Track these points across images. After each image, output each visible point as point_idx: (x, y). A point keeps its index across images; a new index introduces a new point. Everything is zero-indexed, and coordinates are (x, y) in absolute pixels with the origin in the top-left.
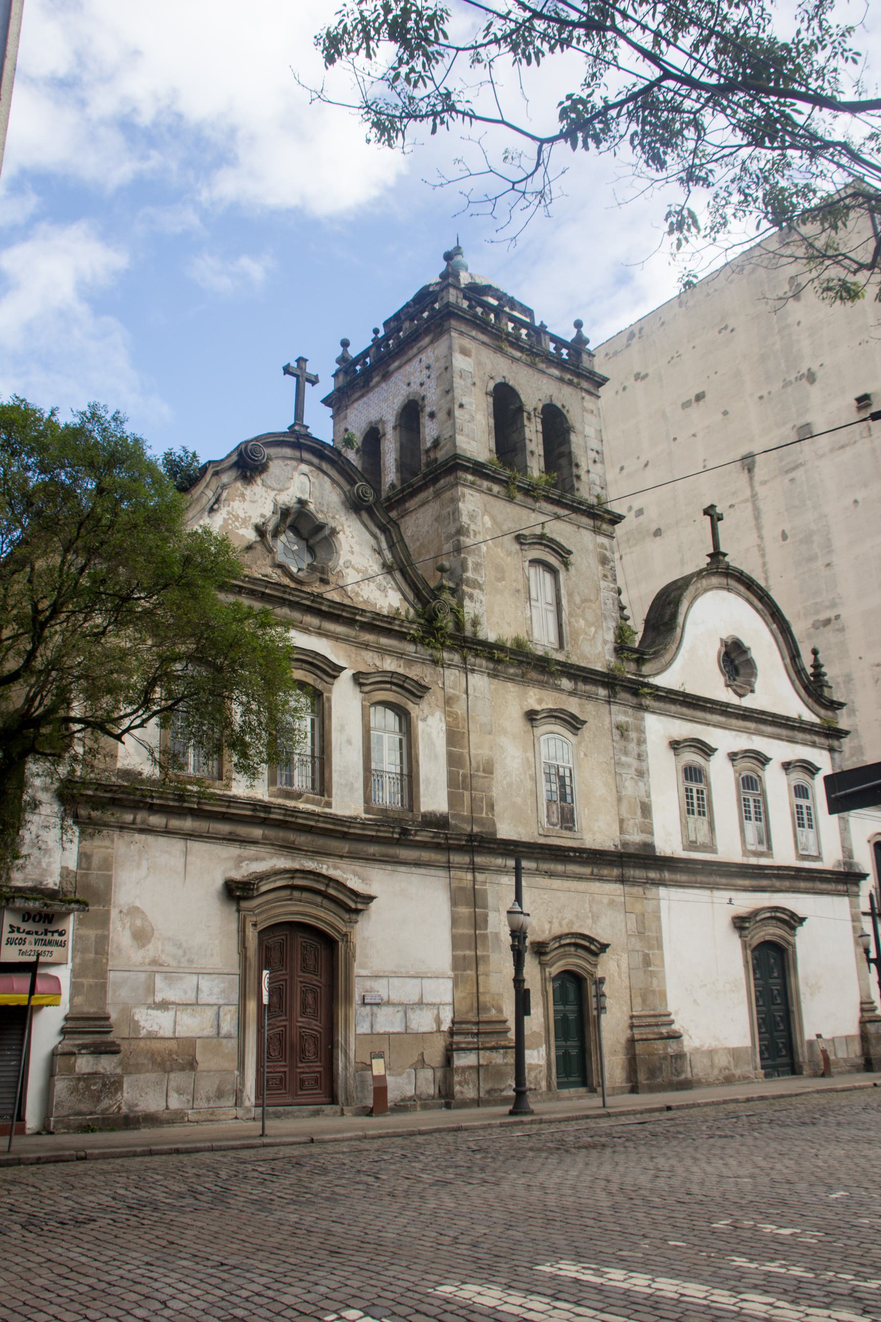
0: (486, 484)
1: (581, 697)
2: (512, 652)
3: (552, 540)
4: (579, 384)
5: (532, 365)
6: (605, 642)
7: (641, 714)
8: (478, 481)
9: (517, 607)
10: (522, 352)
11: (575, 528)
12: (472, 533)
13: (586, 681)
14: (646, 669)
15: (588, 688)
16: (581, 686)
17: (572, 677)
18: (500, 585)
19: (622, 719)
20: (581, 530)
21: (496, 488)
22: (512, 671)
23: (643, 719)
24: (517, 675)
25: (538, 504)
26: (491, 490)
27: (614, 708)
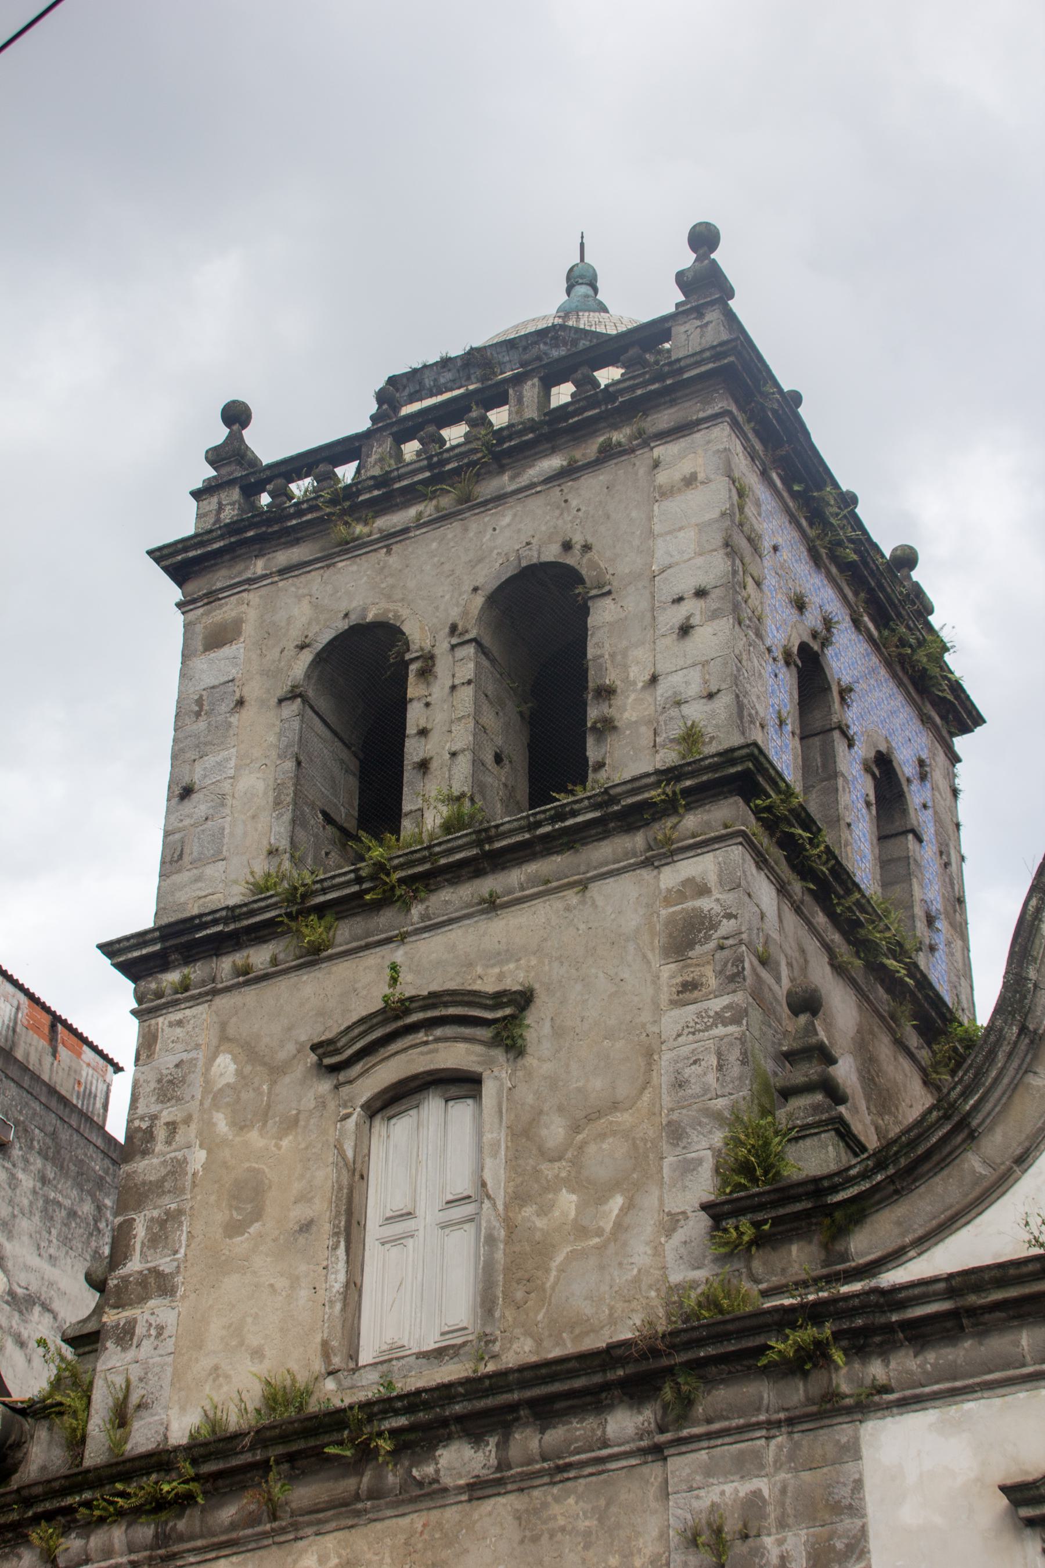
0: (226, 965)
1: (525, 1483)
2: (263, 1437)
3: (435, 999)
4: (640, 433)
5: (469, 505)
6: (672, 1222)
7: (843, 1432)
8: (196, 972)
9: (295, 1281)
10: (423, 497)
11: (572, 897)
12: (161, 1133)
13: (545, 1412)
14: (862, 1245)
15: (555, 1436)
16: (527, 1441)
17: (474, 1427)
18: (240, 1243)
19: (727, 1492)
20: (594, 888)
21: (259, 956)
22: (228, 1513)
23: (852, 1451)
24: (252, 1520)
25: (416, 911)
26: (244, 971)
27: (682, 1466)
